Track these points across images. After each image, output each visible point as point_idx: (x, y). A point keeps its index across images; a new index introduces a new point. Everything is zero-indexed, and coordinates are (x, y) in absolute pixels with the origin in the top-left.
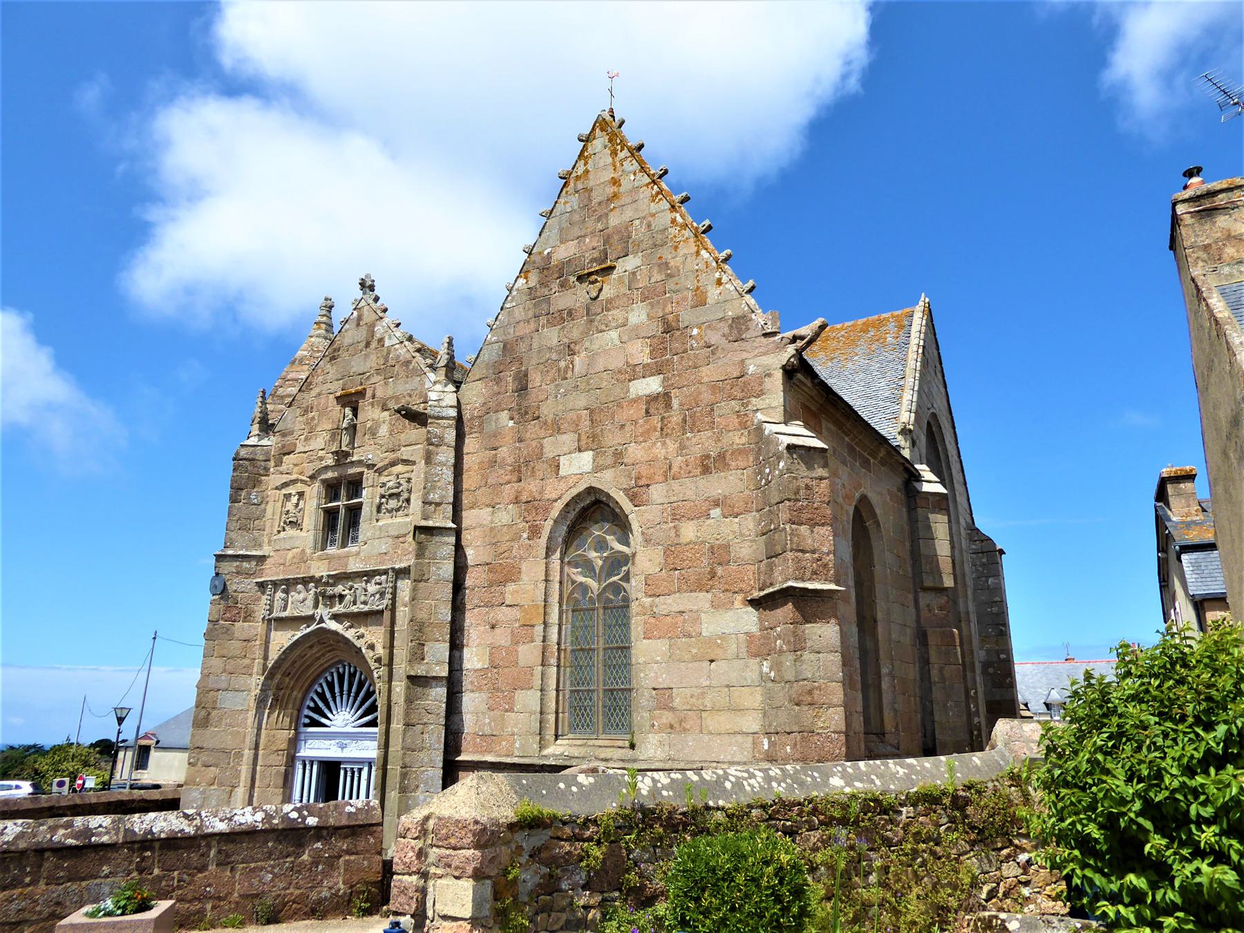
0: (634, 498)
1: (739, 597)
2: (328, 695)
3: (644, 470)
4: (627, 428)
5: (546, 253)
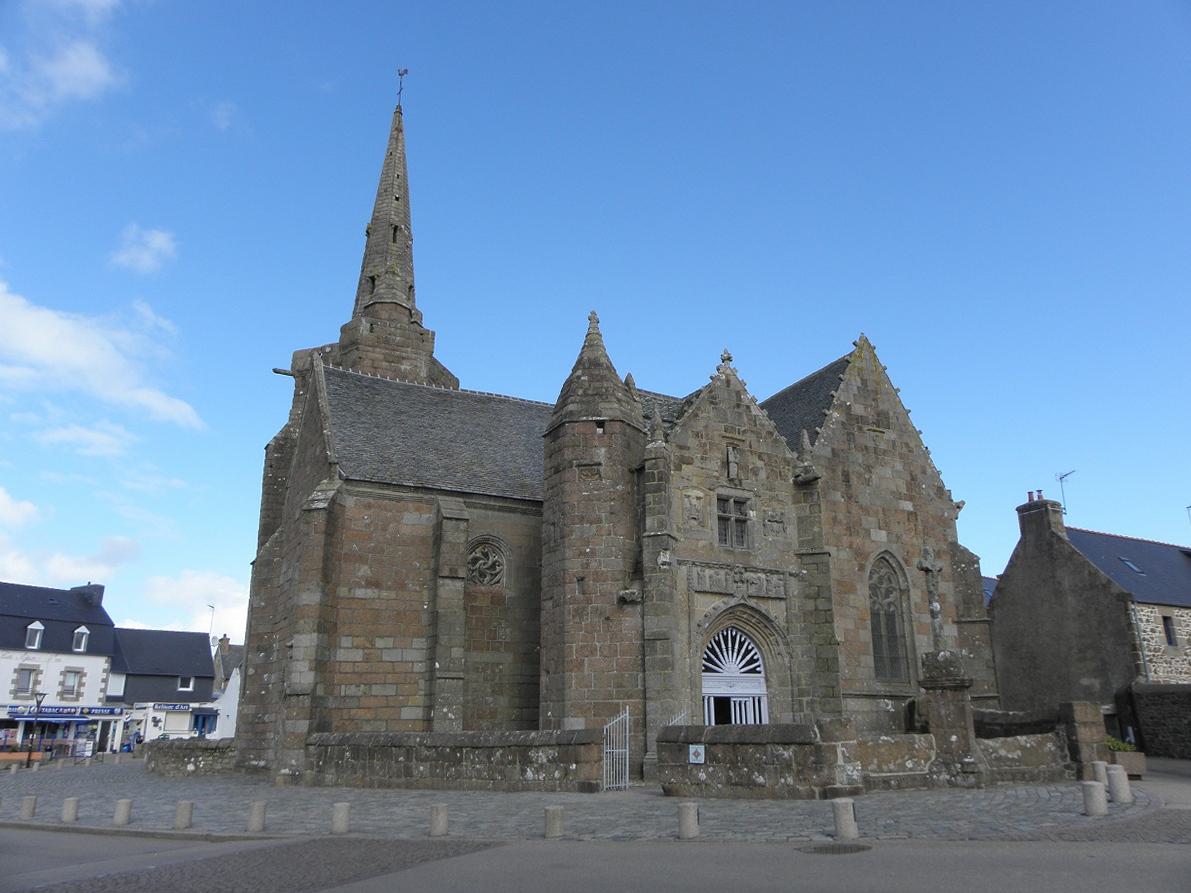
0: (906, 561)
1: (950, 620)
2: (717, 650)
3: (911, 550)
4: (902, 524)
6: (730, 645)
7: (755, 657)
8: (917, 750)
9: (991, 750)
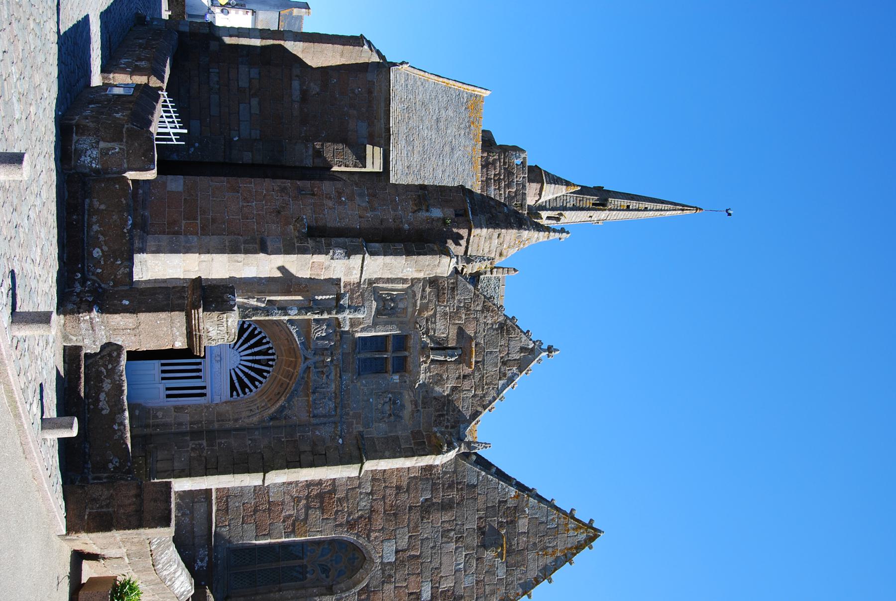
2: (252, 342)
5: (526, 509)
6: (258, 358)
7: (247, 390)
8: (113, 263)
9: (110, 366)
